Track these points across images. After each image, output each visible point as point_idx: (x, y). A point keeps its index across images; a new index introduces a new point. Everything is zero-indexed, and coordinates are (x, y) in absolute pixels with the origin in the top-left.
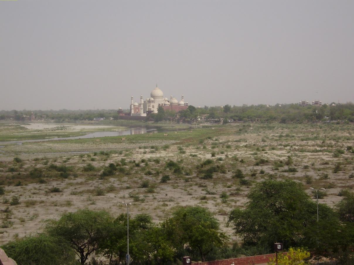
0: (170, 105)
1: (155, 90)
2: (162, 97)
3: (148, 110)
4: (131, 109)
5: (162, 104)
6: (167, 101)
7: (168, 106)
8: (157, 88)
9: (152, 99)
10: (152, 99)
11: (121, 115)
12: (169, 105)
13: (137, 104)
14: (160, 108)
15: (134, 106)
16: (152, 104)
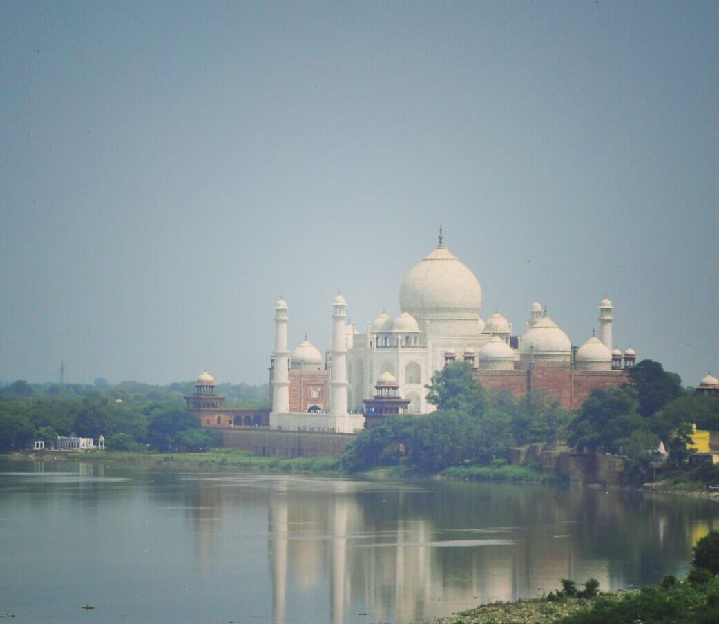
0: (517, 365)
1: (426, 265)
2: (475, 310)
3: (375, 393)
4: (271, 389)
5: (469, 357)
6: (497, 338)
7: (503, 374)
8: (444, 253)
9: (409, 323)
10: (409, 323)
11: (209, 419)
12: (510, 367)
13: (310, 353)
14: (454, 382)
15: (295, 364)
16: (405, 356)
